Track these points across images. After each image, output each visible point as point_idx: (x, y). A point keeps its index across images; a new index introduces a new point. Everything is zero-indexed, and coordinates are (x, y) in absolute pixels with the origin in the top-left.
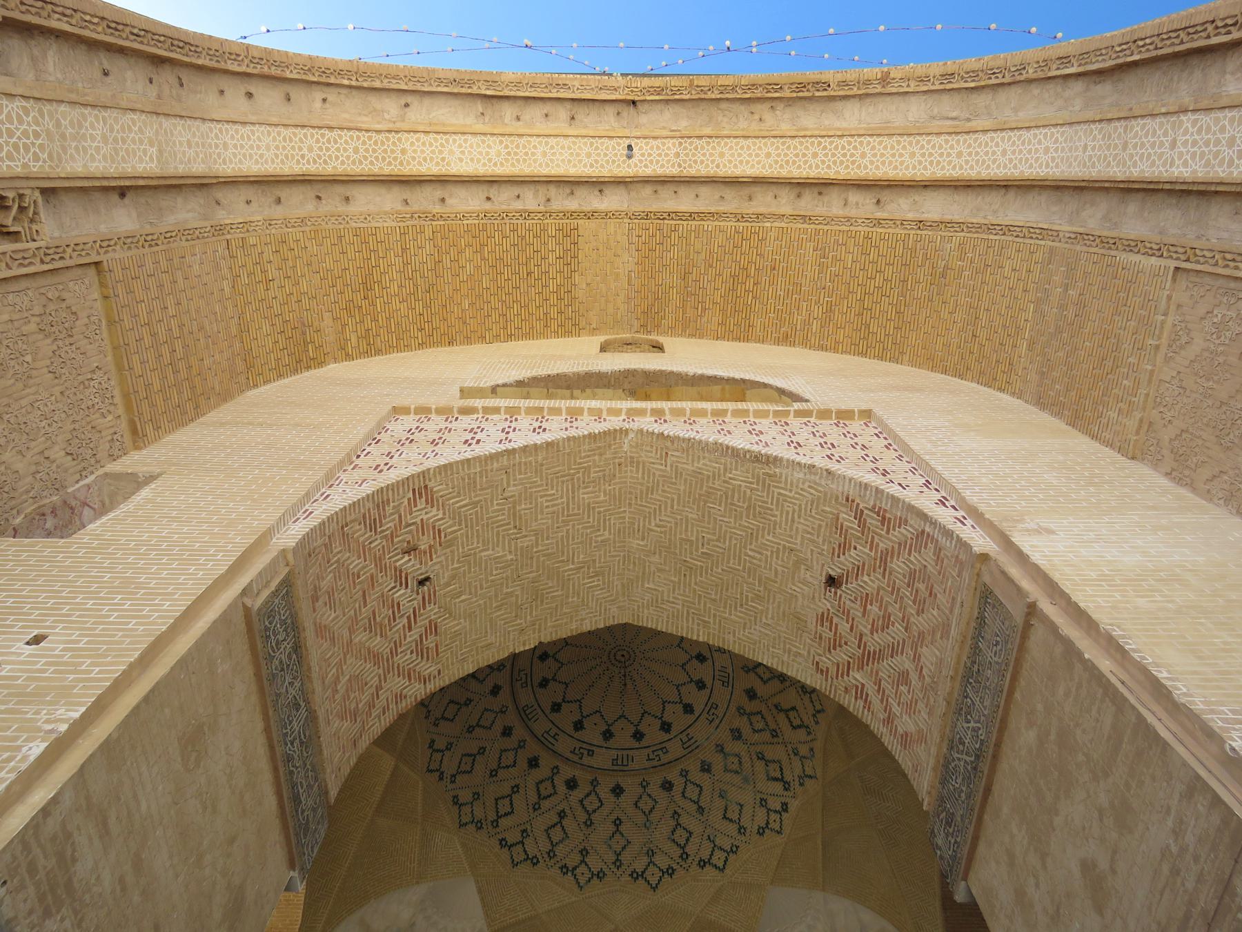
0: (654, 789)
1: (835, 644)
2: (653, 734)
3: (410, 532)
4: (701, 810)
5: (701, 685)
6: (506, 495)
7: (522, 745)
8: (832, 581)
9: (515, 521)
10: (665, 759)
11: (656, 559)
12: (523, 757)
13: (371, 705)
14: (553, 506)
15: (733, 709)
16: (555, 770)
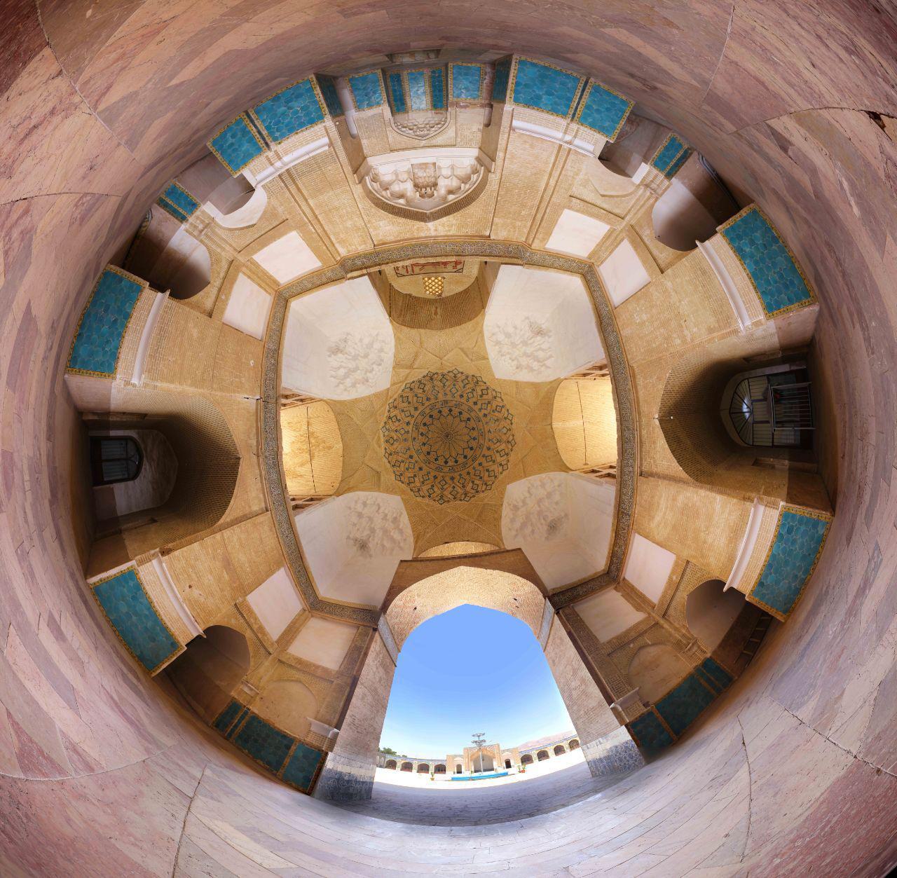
2: (435, 413)
4: (416, 395)
7: (480, 410)
12: (479, 406)
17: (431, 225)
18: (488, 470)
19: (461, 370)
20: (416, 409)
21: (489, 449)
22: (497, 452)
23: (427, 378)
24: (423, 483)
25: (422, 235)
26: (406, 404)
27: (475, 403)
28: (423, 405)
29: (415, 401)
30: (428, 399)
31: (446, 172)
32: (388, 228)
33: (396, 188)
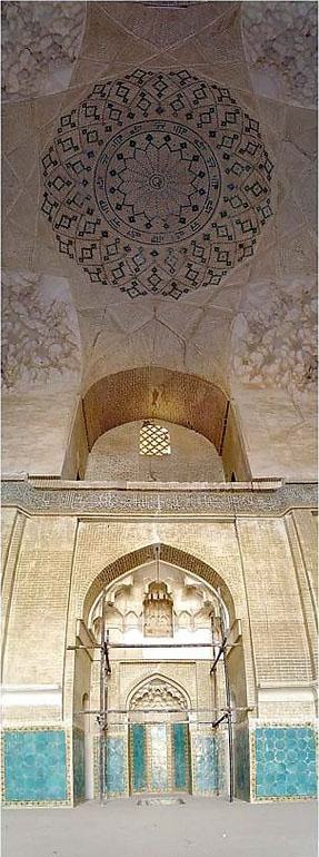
4: (204, 261)
5: (202, 192)
15: (221, 200)
18: (97, 117)
20: (207, 237)
21: (90, 154)
22: (76, 148)
24: (212, 110)
29: (207, 251)
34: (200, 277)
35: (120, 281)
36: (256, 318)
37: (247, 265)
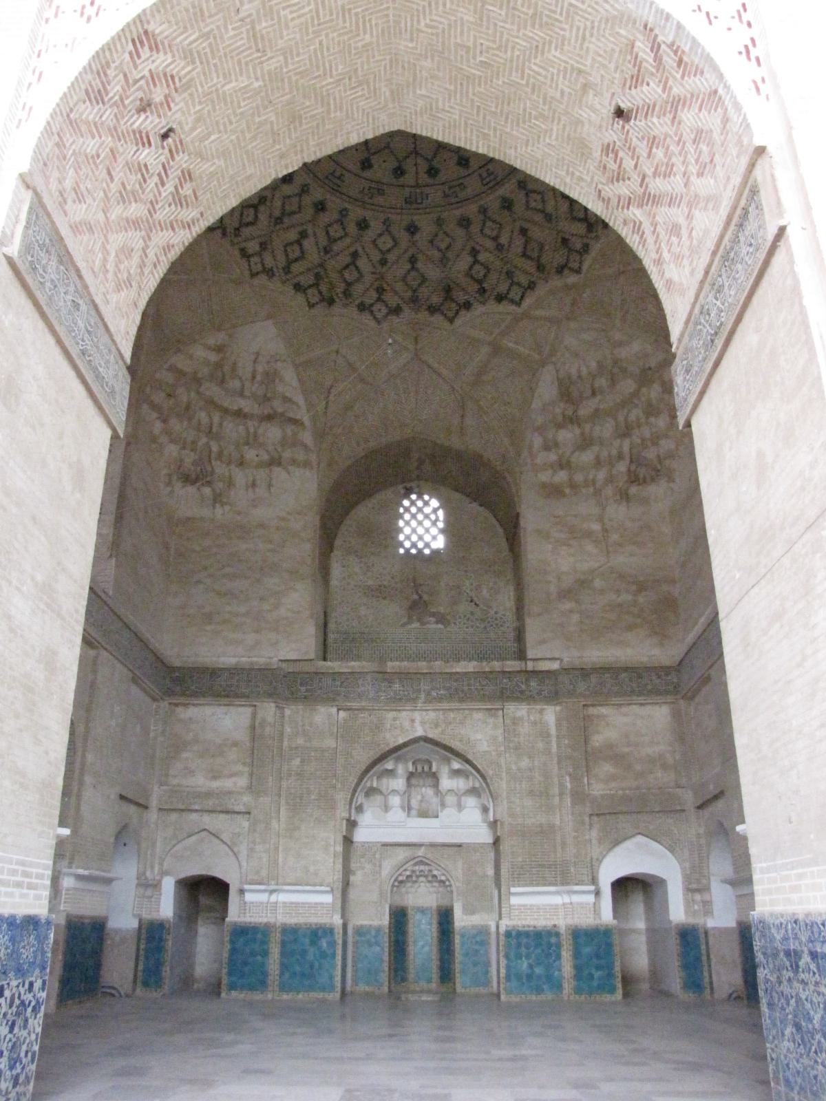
0: (451, 226)
1: (619, 177)
3: (140, 88)
4: (500, 247)
6: (242, 15)
8: (619, 113)
9: (256, 44)
10: (462, 195)
11: (427, 64)
13: (142, 266)
14: (299, 17)
16: (343, 213)
17: (420, 732)
19: (366, 319)
20: (507, 204)
23: (461, 297)
25: (432, 715)
26: (536, 233)
27: (320, 207)
28: (483, 211)
30: (465, 222)
31: (395, 801)
32: (479, 736)
33: (460, 784)
34: (493, 277)
35: (358, 289)
36: (574, 371)
37: (568, 288)
